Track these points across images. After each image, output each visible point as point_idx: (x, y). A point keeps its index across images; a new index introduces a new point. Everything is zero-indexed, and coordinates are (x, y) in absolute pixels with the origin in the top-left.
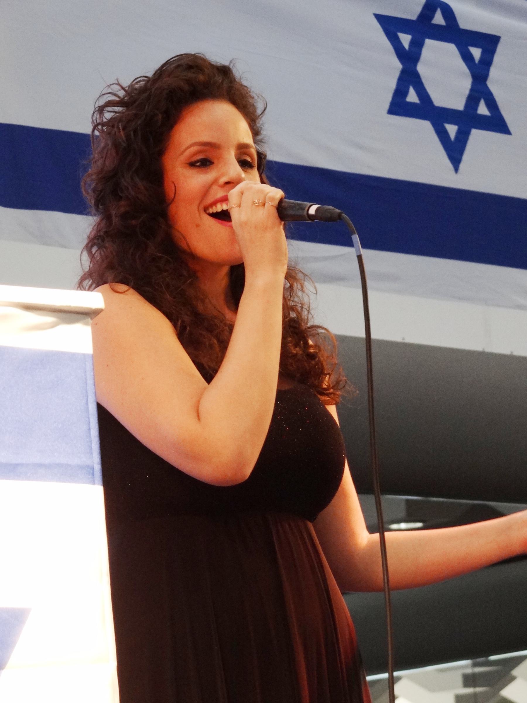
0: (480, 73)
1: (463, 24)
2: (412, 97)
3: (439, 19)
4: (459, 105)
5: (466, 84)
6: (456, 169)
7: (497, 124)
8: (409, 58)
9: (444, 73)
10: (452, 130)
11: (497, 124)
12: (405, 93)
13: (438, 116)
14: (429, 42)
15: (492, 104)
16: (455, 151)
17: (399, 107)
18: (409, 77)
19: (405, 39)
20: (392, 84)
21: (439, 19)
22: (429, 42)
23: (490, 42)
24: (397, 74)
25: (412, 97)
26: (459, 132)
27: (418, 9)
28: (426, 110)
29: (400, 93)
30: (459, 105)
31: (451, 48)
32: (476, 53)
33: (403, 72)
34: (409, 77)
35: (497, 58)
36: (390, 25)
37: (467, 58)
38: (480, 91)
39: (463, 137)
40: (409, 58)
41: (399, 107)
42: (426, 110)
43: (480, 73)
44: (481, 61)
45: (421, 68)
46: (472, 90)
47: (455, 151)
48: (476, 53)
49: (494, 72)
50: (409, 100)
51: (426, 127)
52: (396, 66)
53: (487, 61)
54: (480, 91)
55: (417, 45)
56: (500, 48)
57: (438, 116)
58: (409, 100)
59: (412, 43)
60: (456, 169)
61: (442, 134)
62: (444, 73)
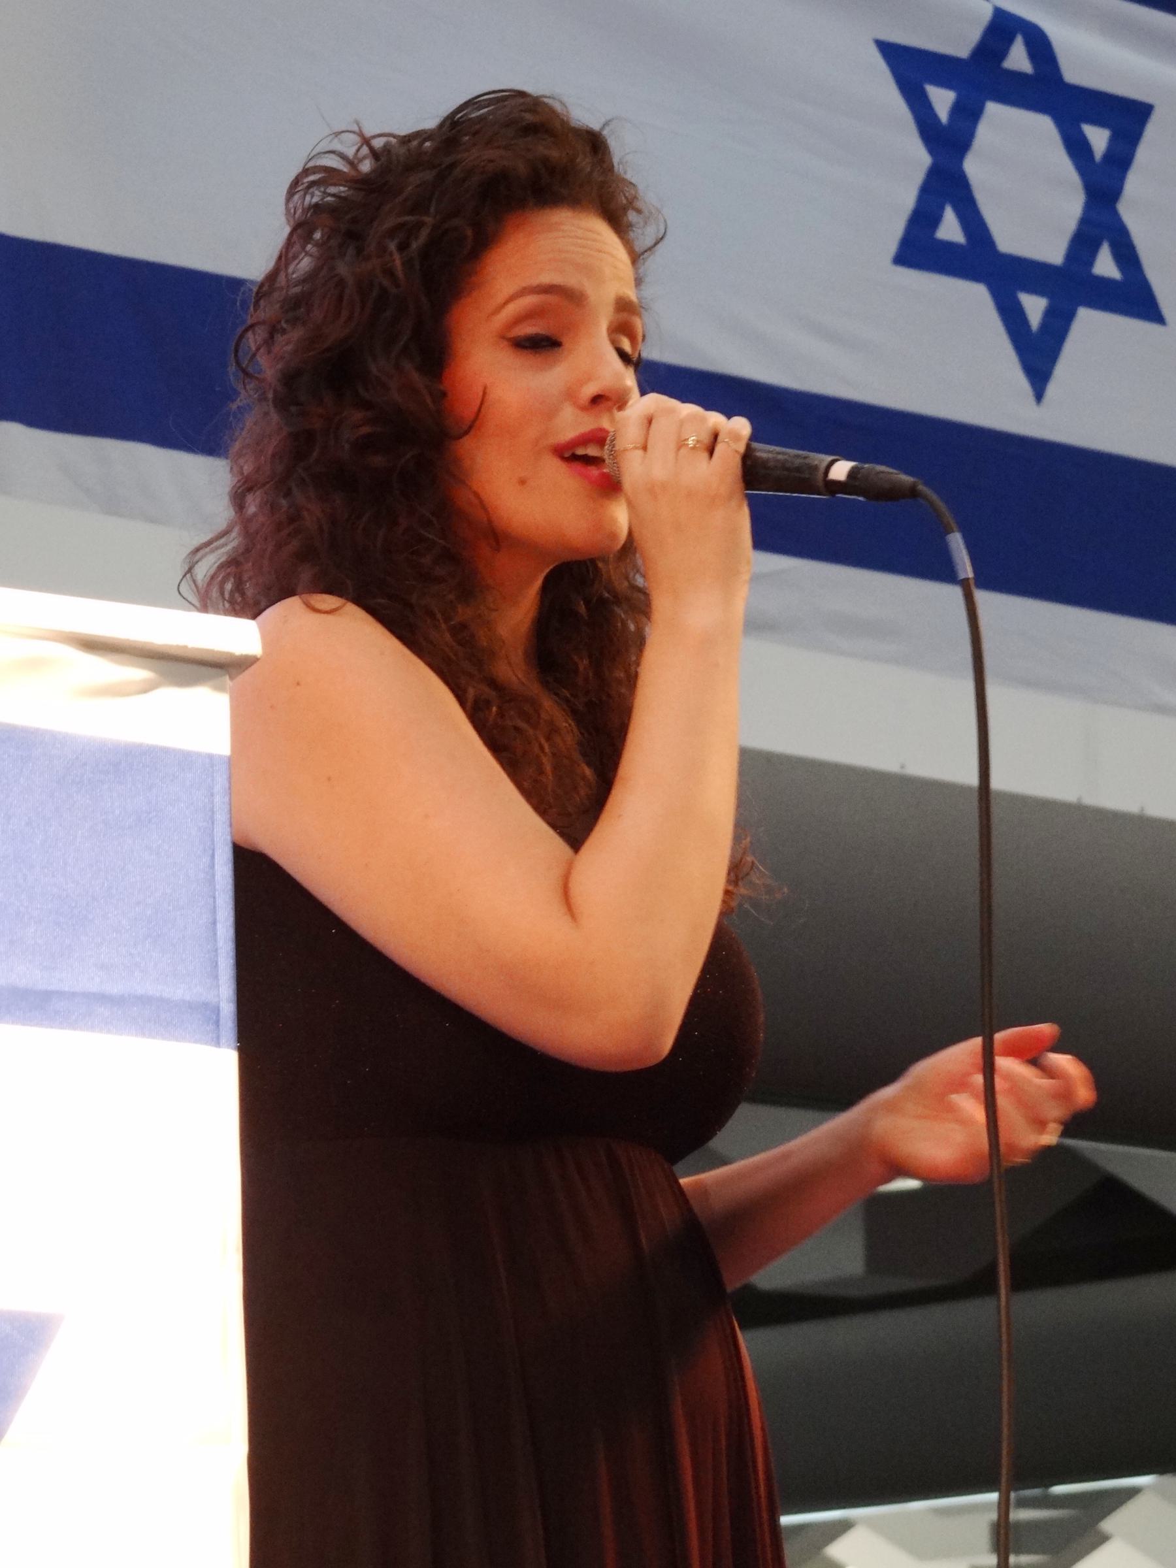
0: (1103, 183)
1: (1073, 73)
2: (950, 229)
3: (1018, 59)
4: (1053, 252)
5: (1070, 205)
6: (1039, 396)
7: (1135, 298)
8: (948, 143)
9: (1025, 182)
10: (1034, 307)
11: (1135, 298)
12: (935, 220)
13: (1004, 276)
14: (994, 110)
15: (1127, 255)
16: (1038, 355)
17: (918, 249)
18: (946, 185)
19: (942, 100)
20: (907, 198)
21: (1018, 59)
22: (994, 110)
23: (1129, 117)
24: (919, 177)
25: (950, 229)
26: (1049, 314)
27: (974, 35)
28: (979, 260)
29: (923, 219)
30: (1053, 252)
31: (1042, 126)
32: (1098, 138)
33: (934, 173)
34: (946, 185)
35: (1143, 154)
36: (910, 67)
37: (1077, 148)
38: (1101, 223)
40: (948, 143)
41: (918, 249)
42: (979, 260)
43: (1103, 183)
44: (1109, 156)
45: (972, 166)
46: (1084, 221)
47: (1038, 355)
48: (1098, 138)
49: (1135, 185)
50: (943, 236)
51: (973, 298)
52: (920, 158)
53: (1121, 158)
54: (1101, 223)
55: (968, 114)
56: (1151, 131)
57: (1004, 276)
58: (943, 236)
59: (957, 109)
60: (1039, 396)
61: (1012, 317)
62: (1025, 182)
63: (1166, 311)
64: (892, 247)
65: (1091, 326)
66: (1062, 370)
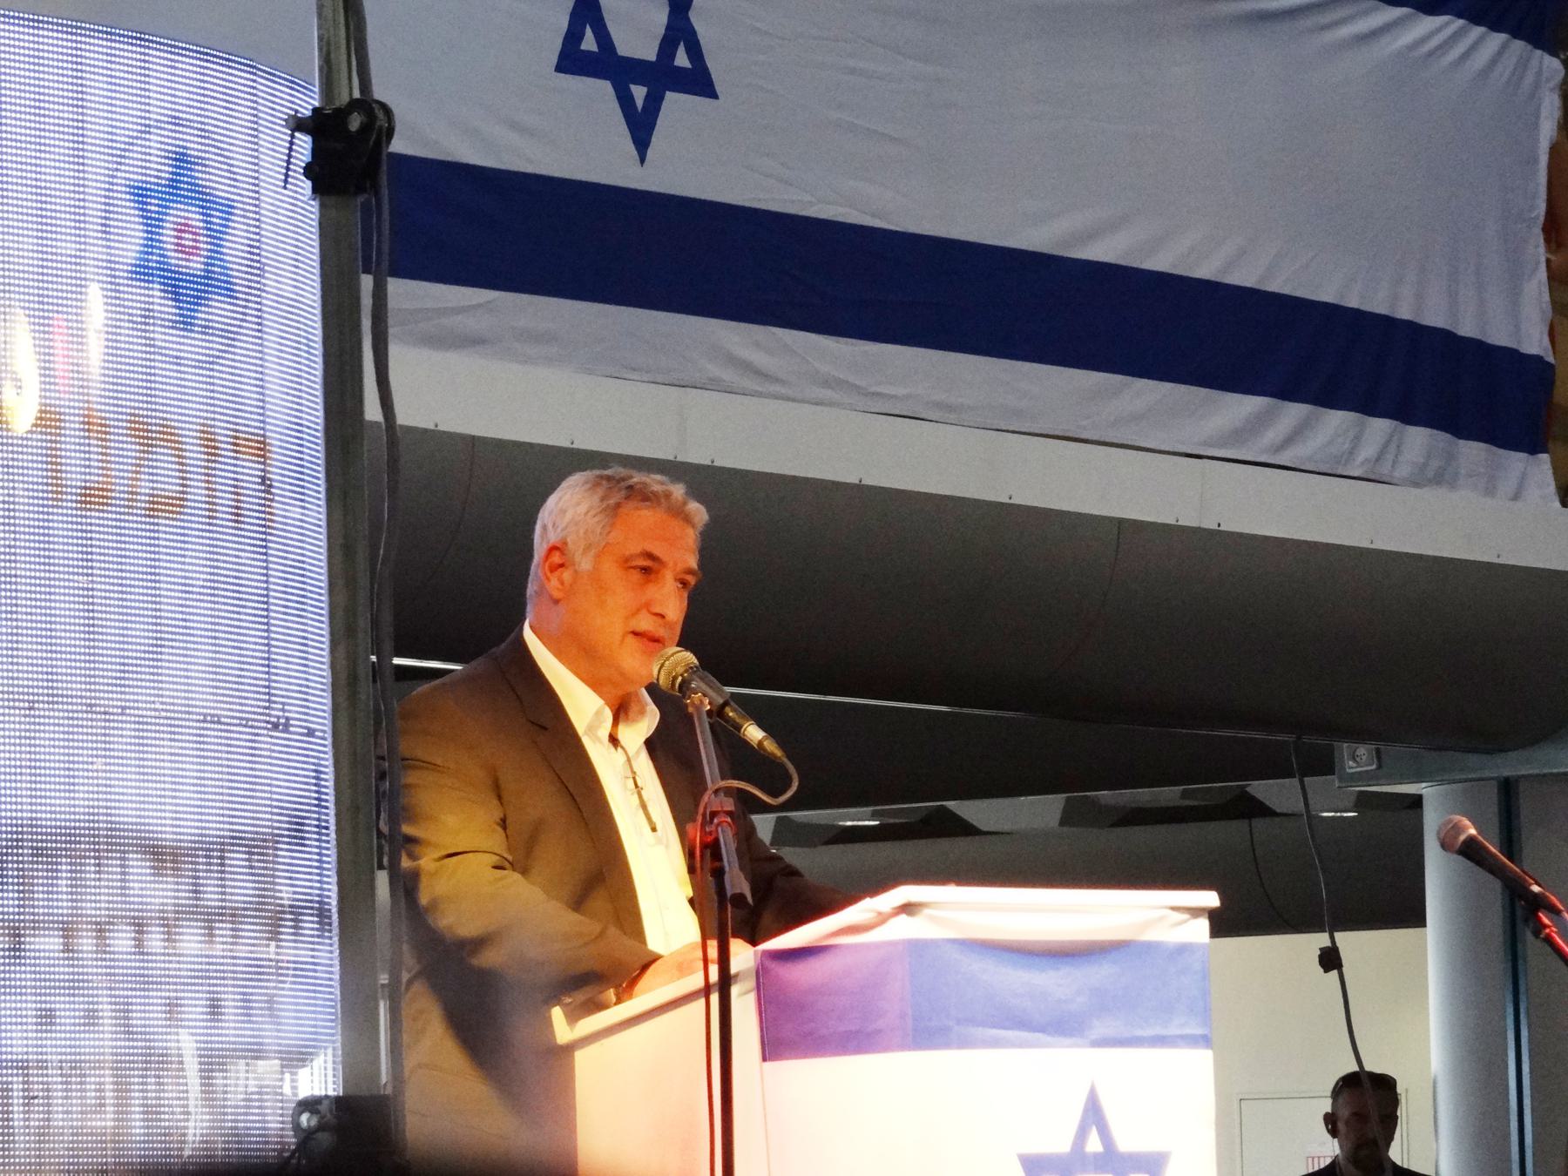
2: (589, 43)
4: (649, 53)
5: (659, 18)
6: (642, 160)
7: (700, 83)
10: (639, 93)
11: (700, 83)
15: (695, 52)
16: (641, 127)
17: (571, 61)
20: (563, 23)
25: (589, 43)
29: (573, 36)
30: (649, 53)
38: (679, 31)
39: (654, 102)
41: (571, 61)
46: (668, 28)
47: (641, 127)
51: (604, 88)
54: (679, 31)
60: (642, 160)
61: (625, 100)
63: (718, 89)
64: (554, 59)
65: (674, 102)
66: (656, 139)
